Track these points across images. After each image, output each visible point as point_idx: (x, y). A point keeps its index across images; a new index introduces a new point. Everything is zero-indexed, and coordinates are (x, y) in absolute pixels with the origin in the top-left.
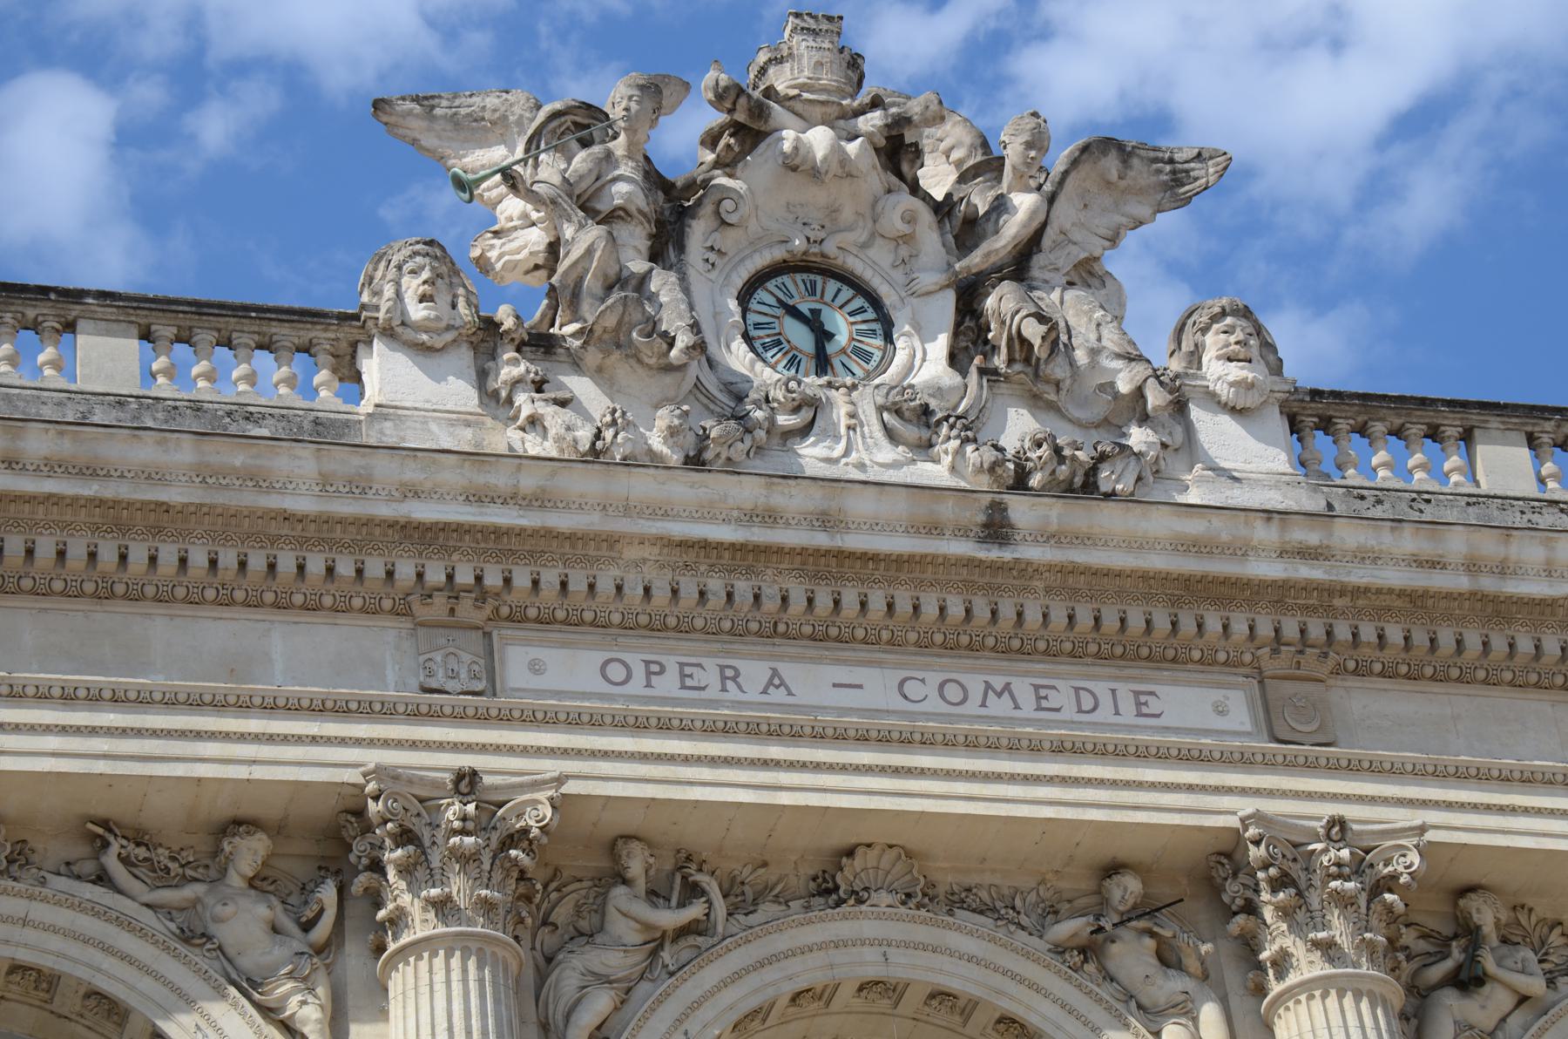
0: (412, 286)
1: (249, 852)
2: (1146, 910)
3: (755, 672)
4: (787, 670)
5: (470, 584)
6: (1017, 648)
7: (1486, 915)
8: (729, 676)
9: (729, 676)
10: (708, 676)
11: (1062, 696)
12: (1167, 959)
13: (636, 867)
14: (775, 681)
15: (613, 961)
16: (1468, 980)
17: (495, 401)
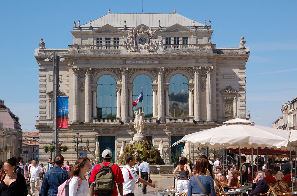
0: (123, 44)
1: (117, 70)
2: (154, 70)
3: (137, 62)
4: (138, 61)
5: (126, 59)
6: (148, 60)
7: (169, 69)
8: (136, 62)
9: (136, 62)
10: (135, 62)
11: (150, 62)
12: (154, 72)
13: (132, 69)
14: (138, 62)
15: (131, 74)
16: (167, 72)
17: (127, 49)
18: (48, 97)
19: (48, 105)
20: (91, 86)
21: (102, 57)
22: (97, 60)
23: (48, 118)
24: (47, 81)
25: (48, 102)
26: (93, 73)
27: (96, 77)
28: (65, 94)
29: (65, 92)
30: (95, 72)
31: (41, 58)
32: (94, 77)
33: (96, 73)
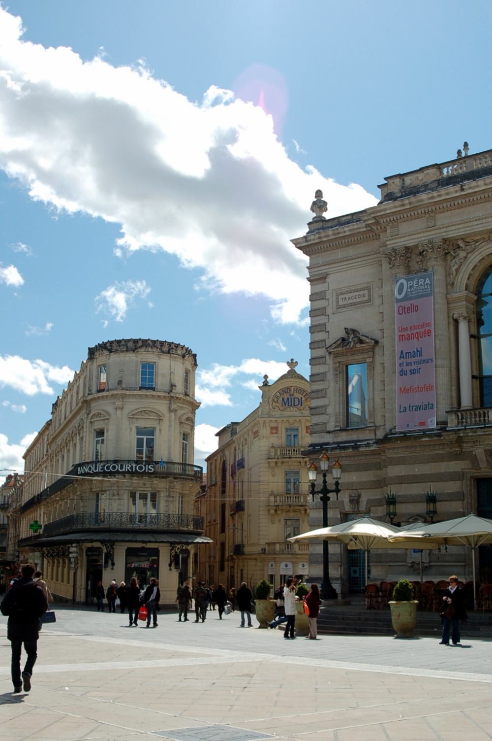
18: (329, 360)
19: (332, 384)
20: (448, 304)
21: (471, 191)
22: (460, 207)
23: (331, 427)
24: (329, 311)
25: (330, 376)
26: (454, 257)
27: (463, 269)
28: (377, 342)
29: (377, 335)
30: (460, 252)
31: (309, 243)
32: (457, 270)
33: (462, 254)
